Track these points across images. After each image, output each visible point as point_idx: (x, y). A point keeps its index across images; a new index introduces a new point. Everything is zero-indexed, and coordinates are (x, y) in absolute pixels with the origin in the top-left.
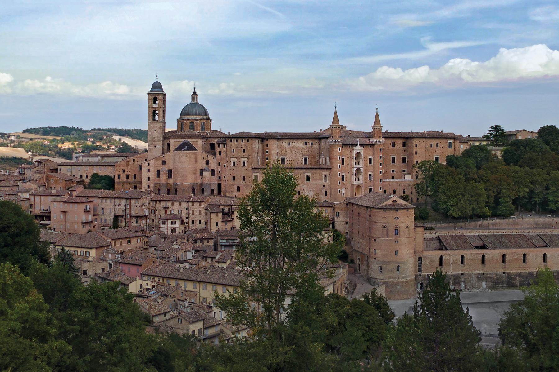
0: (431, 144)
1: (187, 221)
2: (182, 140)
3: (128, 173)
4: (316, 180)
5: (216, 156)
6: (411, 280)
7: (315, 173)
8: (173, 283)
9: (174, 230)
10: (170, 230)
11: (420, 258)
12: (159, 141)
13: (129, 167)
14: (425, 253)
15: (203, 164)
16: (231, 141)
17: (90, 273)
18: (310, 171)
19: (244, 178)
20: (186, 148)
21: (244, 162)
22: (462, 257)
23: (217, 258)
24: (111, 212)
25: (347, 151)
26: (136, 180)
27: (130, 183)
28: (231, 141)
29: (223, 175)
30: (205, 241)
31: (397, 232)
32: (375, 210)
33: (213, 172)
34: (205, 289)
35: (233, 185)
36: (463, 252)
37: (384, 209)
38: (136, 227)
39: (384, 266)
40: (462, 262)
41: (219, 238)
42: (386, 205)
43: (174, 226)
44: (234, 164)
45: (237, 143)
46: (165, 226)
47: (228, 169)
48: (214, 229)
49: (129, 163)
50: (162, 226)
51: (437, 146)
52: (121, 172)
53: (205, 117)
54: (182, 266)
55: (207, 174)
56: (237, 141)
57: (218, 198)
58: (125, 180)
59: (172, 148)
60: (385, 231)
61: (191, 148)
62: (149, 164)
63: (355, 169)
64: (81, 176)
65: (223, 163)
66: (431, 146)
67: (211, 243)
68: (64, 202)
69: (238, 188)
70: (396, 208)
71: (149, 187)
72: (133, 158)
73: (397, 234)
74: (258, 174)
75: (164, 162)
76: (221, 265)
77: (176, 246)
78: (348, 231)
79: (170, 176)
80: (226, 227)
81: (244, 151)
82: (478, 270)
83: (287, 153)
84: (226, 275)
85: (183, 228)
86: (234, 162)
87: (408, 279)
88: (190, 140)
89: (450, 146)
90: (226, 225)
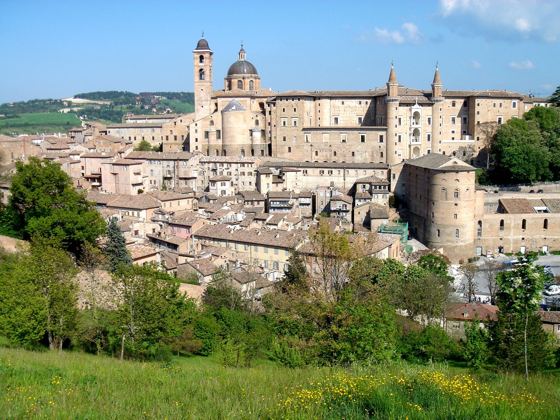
0: (495, 104)
1: (236, 183)
3: (176, 134)
4: (371, 140)
5: (265, 115)
6: (470, 244)
7: (371, 133)
8: (223, 244)
9: (224, 192)
10: (219, 193)
11: (480, 222)
12: (207, 100)
13: (176, 128)
14: (486, 217)
15: (252, 125)
17: (141, 233)
20: (234, 108)
21: (295, 122)
22: (524, 221)
23: (268, 220)
24: (160, 173)
25: (404, 110)
30: (256, 203)
31: (457, 195)
33: (263, 132)
34: (256, 250)
35: (284, 146)
36: (524, 216)
37: (444, 171)
38: (185, 188)
39: (441, 230)
40: (524, 227)
41: (270, 200)
42: (446, 167)
43: (223, 188)
46: (215, 188)
47: (278, 129)
48: (264, 190)
50: (211, 187)
51: (501, 106)
52: (168, 133)
53: (253, 75)
54: (232, 227)
55: (257, 135)
57: (268, 158)
58: (173, 141)
59: (220, 108)
60: (444, 194)
61: (239, 108)
62: (196, 125)
63: (413, 130)
64: (130, 138)
65: (273, 123)
66: (494, 106)
67: (262, 204)
68: (114, 164)
69: (290, 148)
70: (456, 170)
71: (197, 148)
72: (180, 118)
73: (457, 196)
75: (212, 123)
76: (272, 227)
77: (225, 208)
78: (404, 194)
80: (277, 188)
81: (295, 111)
82: (539, 234)
83: (341, 112)
84: (278, 237)
85: (233, 190)
86: (284, 122)
87: (467, 243)
89: (514, 106)
90: (277, 186)
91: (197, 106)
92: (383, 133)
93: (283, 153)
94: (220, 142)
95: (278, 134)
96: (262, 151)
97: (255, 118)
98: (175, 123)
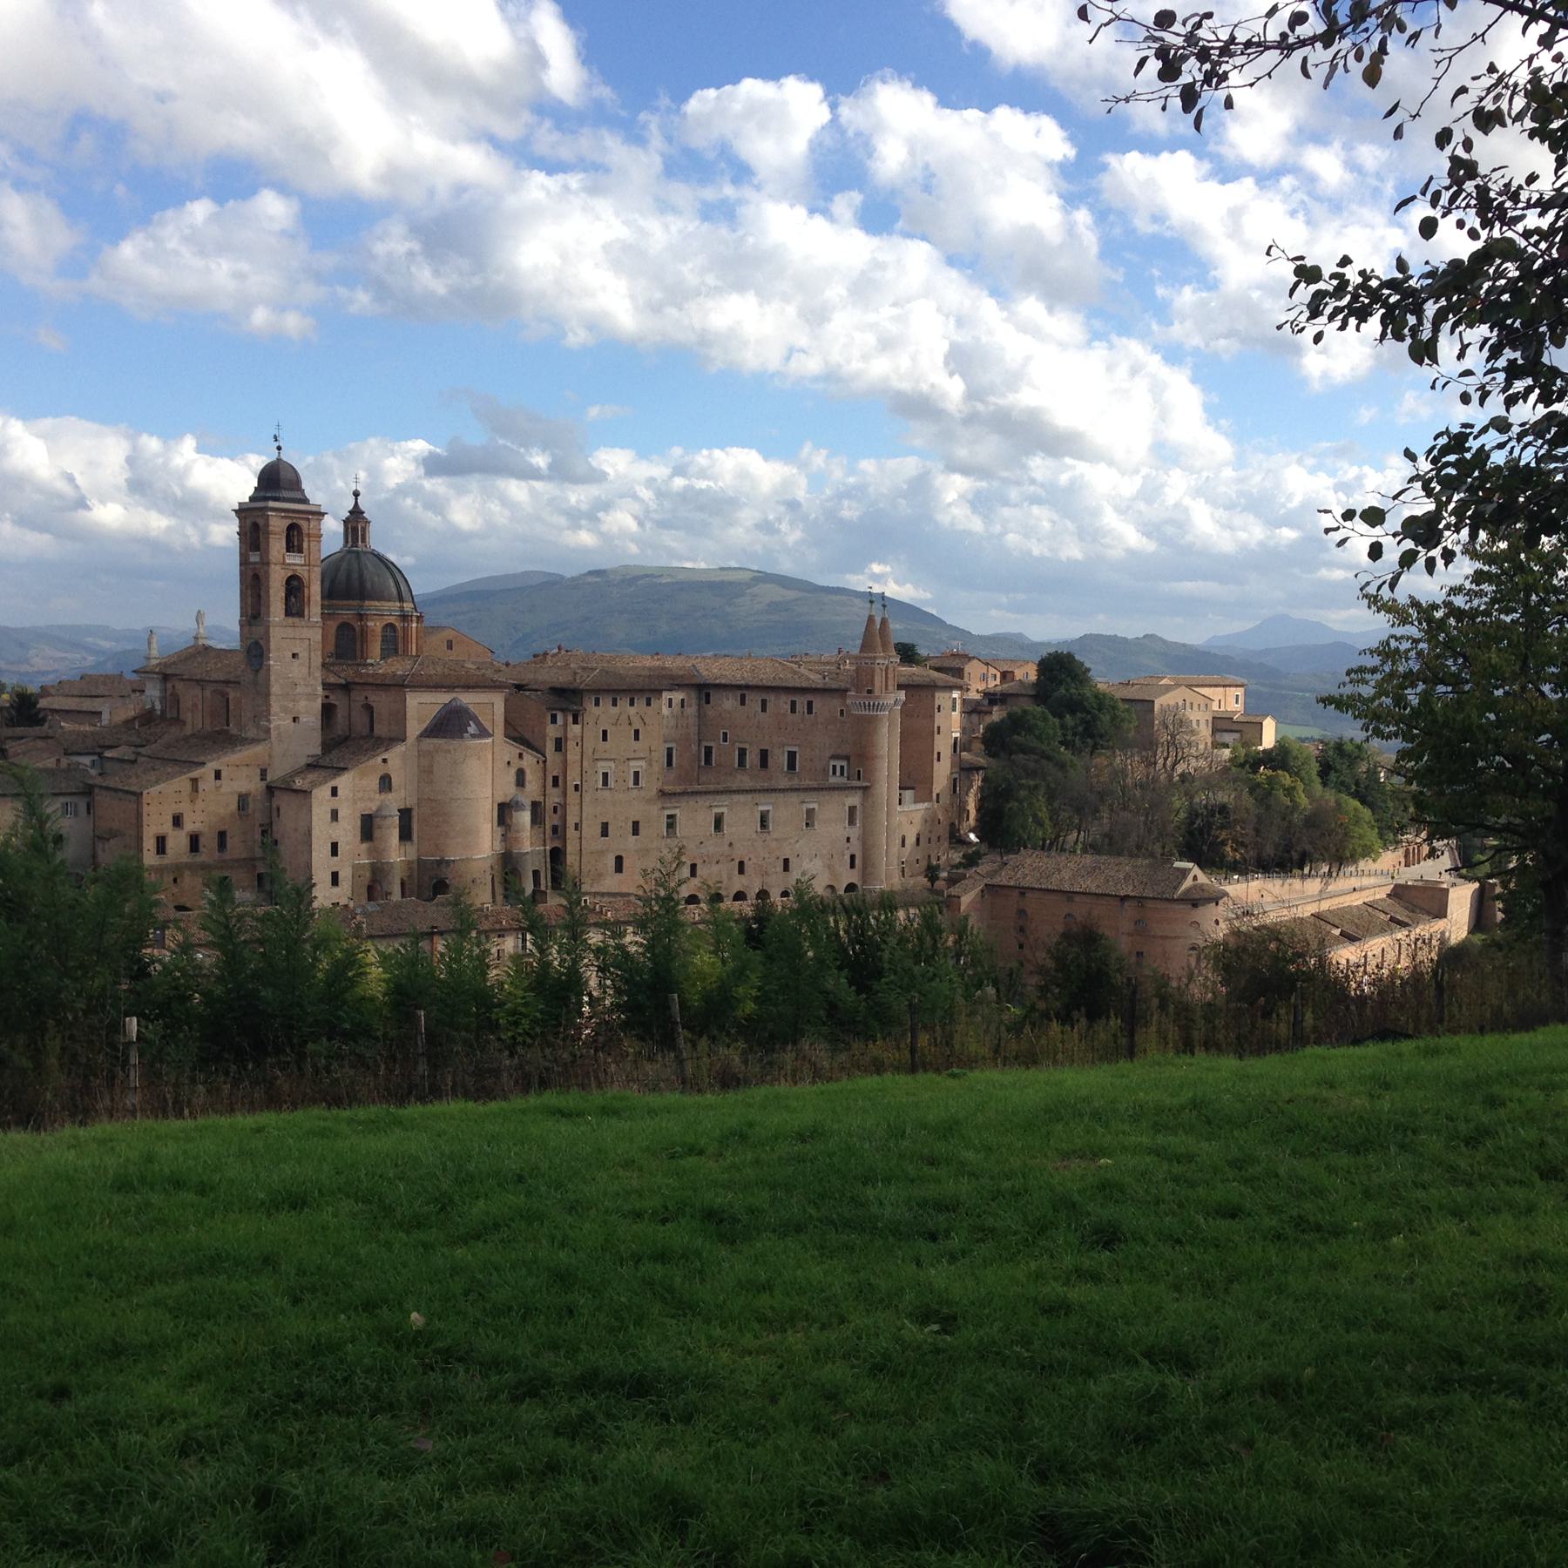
2: (444, 698)
12: (311, 696)
13: (200, 805)
16: (597, 704)
18: (813, 796)
19: (636, 828)
20: (472, 729)
21: (636, 774)
26: (227, 856)
27: (204, 867)
28: (597, 704)
29: (571, 820)
32: (1159, 905)
35: (602, 853)
44: (605, 783)
45: (614, 710)
47: (587, 798)
49: (201, 786)
52: (167, 828)
55: (525, 817)
56: (615, 704)
59: (414, 728)
62: (334, 792)
65: (573, 778)
69: (619, 860)
72: (212, 766)
74: (677, 812)
75: (386, 783)
79: (405, 835)
81: (637, 738)
86: (605, 775)
88: (467, 699)
91: (279, 721)
92: (854, 800)
93: (600, 875)
94: (411, 852)
95: (587, 812)
96: (536, 874)
97: (516, 764)
98: (195, 781)
